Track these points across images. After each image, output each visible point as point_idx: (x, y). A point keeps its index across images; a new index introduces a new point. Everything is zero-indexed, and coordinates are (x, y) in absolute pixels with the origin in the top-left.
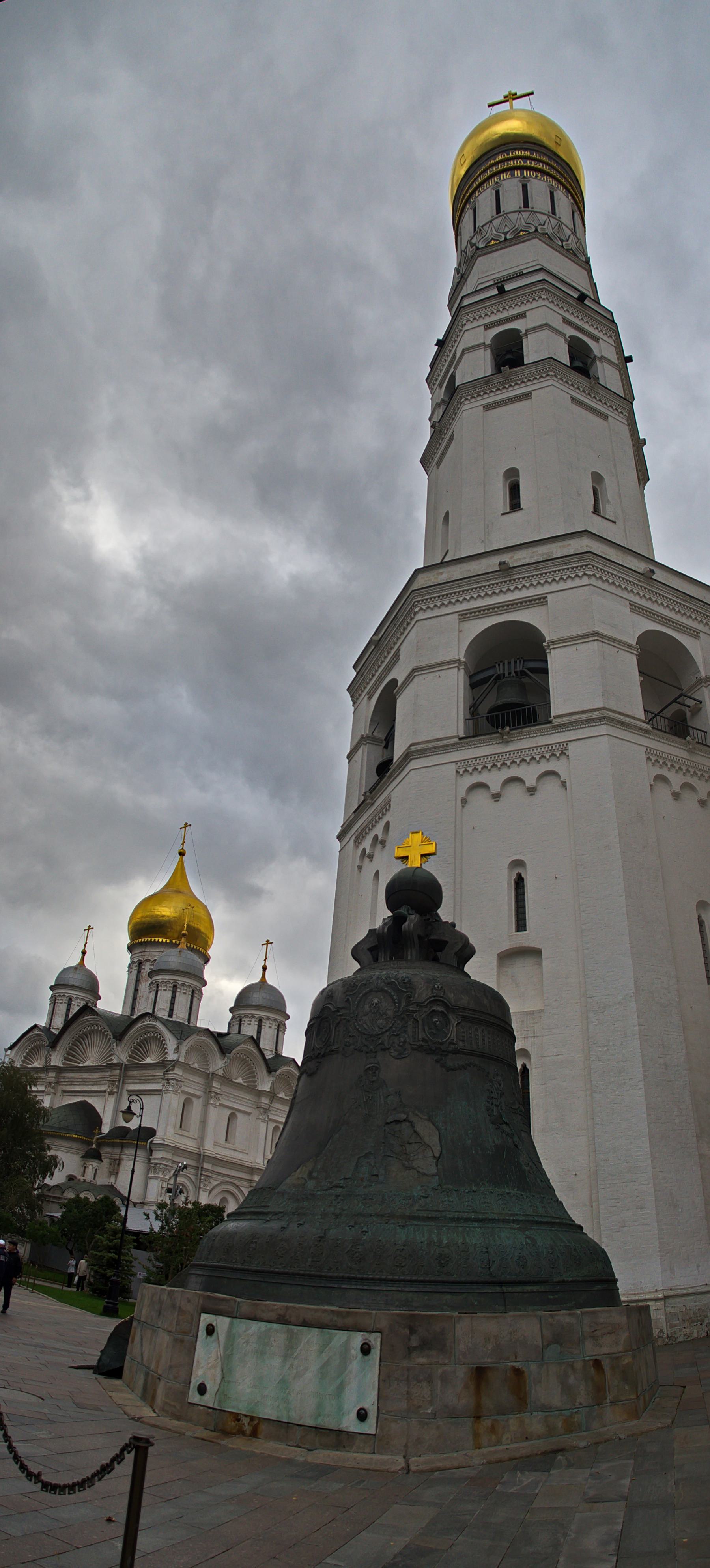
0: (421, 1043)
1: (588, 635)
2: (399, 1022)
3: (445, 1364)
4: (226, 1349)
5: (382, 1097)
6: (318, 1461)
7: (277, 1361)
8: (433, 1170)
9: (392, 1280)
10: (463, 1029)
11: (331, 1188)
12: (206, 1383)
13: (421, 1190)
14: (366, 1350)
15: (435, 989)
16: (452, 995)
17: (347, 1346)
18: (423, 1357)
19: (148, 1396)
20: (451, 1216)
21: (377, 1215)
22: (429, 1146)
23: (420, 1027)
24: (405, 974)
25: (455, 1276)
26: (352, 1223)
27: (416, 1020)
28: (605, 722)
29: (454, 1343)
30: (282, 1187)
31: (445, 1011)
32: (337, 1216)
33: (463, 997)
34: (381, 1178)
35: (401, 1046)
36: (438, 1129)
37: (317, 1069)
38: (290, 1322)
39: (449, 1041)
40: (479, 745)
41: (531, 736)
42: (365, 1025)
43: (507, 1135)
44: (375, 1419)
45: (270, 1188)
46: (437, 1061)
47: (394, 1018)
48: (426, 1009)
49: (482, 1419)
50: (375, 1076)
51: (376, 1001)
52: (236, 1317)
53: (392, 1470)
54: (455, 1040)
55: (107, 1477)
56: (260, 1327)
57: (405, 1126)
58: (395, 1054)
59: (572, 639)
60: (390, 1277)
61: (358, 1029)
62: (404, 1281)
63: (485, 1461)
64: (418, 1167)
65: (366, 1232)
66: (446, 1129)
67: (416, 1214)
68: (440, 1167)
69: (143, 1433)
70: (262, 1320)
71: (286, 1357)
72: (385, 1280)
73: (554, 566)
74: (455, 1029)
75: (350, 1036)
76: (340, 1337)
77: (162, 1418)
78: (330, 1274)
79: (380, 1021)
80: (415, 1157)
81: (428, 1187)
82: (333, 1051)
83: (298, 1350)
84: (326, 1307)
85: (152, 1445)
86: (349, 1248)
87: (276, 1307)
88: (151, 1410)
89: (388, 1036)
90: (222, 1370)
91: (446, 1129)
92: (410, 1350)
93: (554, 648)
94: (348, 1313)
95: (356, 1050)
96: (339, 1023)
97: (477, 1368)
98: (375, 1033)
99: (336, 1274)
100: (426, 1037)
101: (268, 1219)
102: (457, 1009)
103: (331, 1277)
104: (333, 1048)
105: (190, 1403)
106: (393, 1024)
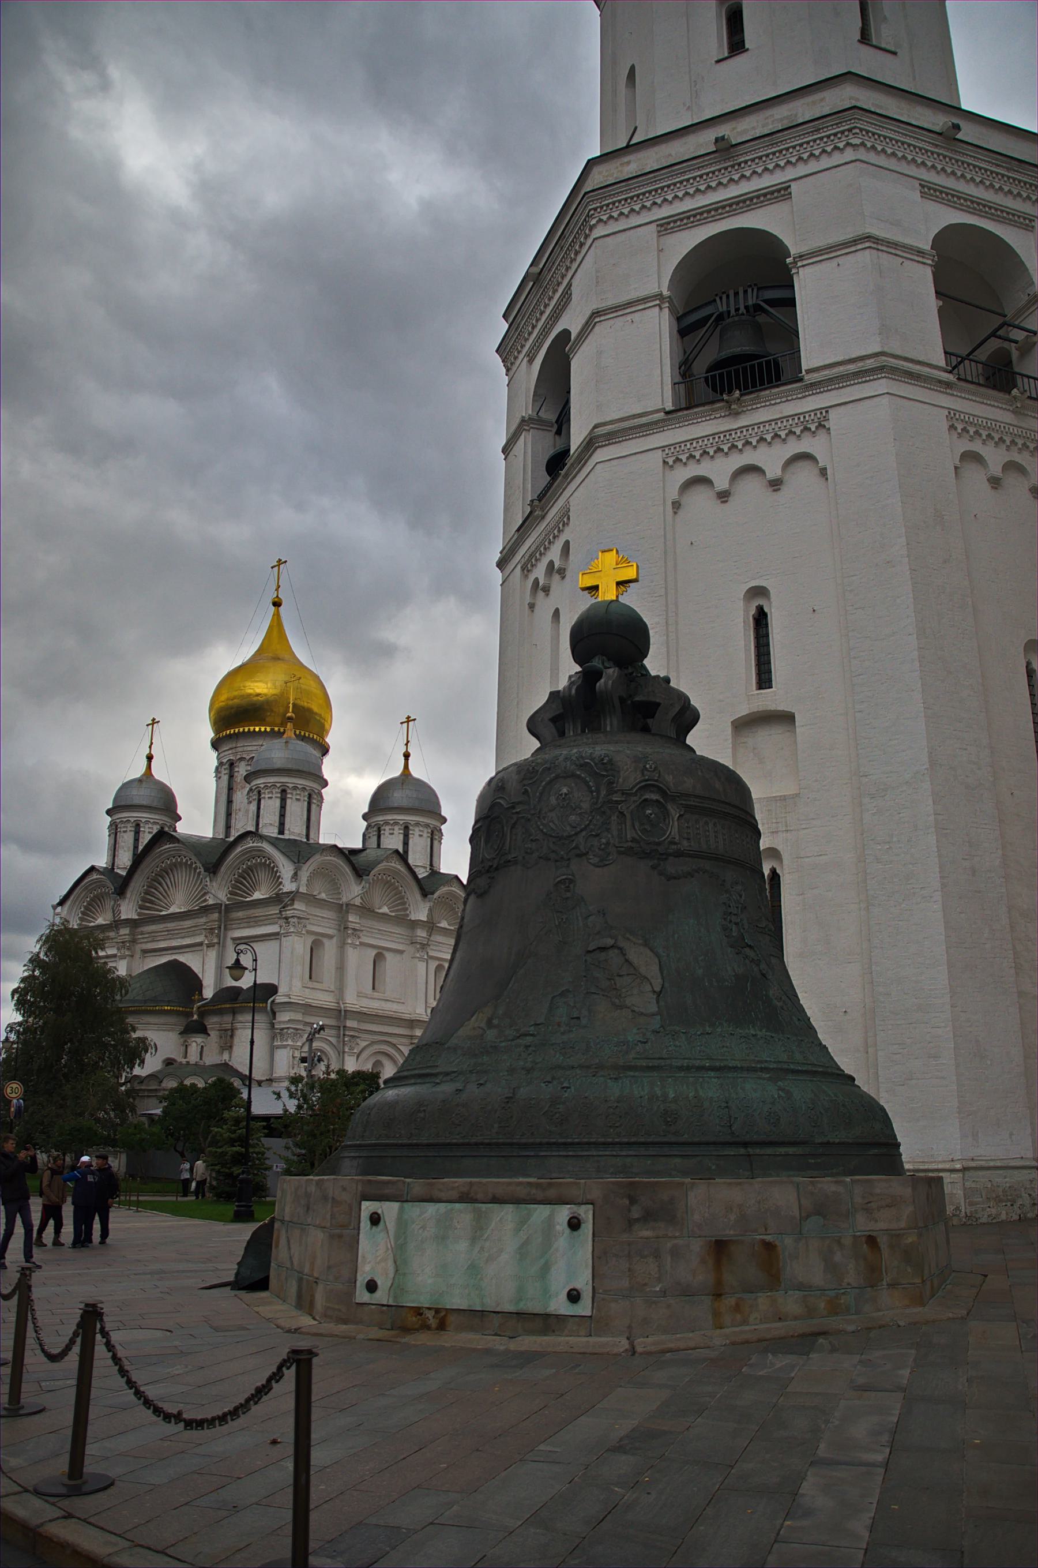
0: (630, 844)
1: (855, 242)
3: (676, 1237)
4: (397, 1237)
5: (580, 918)
6: (523, 1349)
7: (463, 1246)
8: (654, 1008)
9: (604, 1144)
10: (688, 823)
11: (518, 1037)
12: (376, 1279)
13: (637, 1034)
14: (574, 1224)
16: (671, 777)
17: (550, 1222)
19: (304, 1303)
20: (679, 1064)
21: (581, 1067)
22: (646, 978)
23: (629, 823)
24: (604, 752)
25: (686, 1136)
26: (548, 1078)
27: (622, 813)
28: (883, 375)
29: (687, 1212)
30: (454, 1041)
31: (662, 800)
32: (529, 1071)
33: (686, 779)
34: (584, 1021)
35: (603, 850)
36: (657, 955)
37: (490, 887)
38: (476, 1200)
41: (773, 402)
42: (551, 824)
43: (751, 962)
44: (591, 1300)
45: (437, 1043)
46: (653, 867)
47: (591, 812)
48: (635, 798)
49: (723, 1297)
50: (569, 891)
51: (565, 790)
52: (407, 1201)
53: (614, 1352)
54: (677, 838)
55: (265, 1398)
56: (438, 1209)
57: (613, 953)
58: (596, 860)
60: (602, 1140)
61: (542, 831)
62: (620, 1143)
63: (728, 1341)
64: (633, 1005)
65: (568, 1088)
66: (668, 956)
67: (633, 1064)
68: (662, 1003)
69: (303, 1344)
70: (440, 1201)
71: (474, 1240)
72: (594, 1143)
73: (799, 136)
74: (676, 823)
75: (532, 840)
76: (541, 1212)
77: (325, 1325)
78: (524, 1141)
79: (573, 817)
80: (629, 993)
81: (647, 1029)
82: (509, 861)
83: (489, 1232)
84: (521, 1179)
85: (317, 1355)
86: (546, 1109)
87: (457, 1184)
88: (310, 1318)
90: (395, 1262)
91: (668, 956)
92: (631, 1223)
93: (803, 266)
94: (550, 1184)
96: (515, 823)
97: (716, 1241)
98: (565, 834)
99: (531, 1140)
101: (438, 1081)
103: (525, 1144)
104: (509, 857)
105: (357, 1303)
106: (591, 821)
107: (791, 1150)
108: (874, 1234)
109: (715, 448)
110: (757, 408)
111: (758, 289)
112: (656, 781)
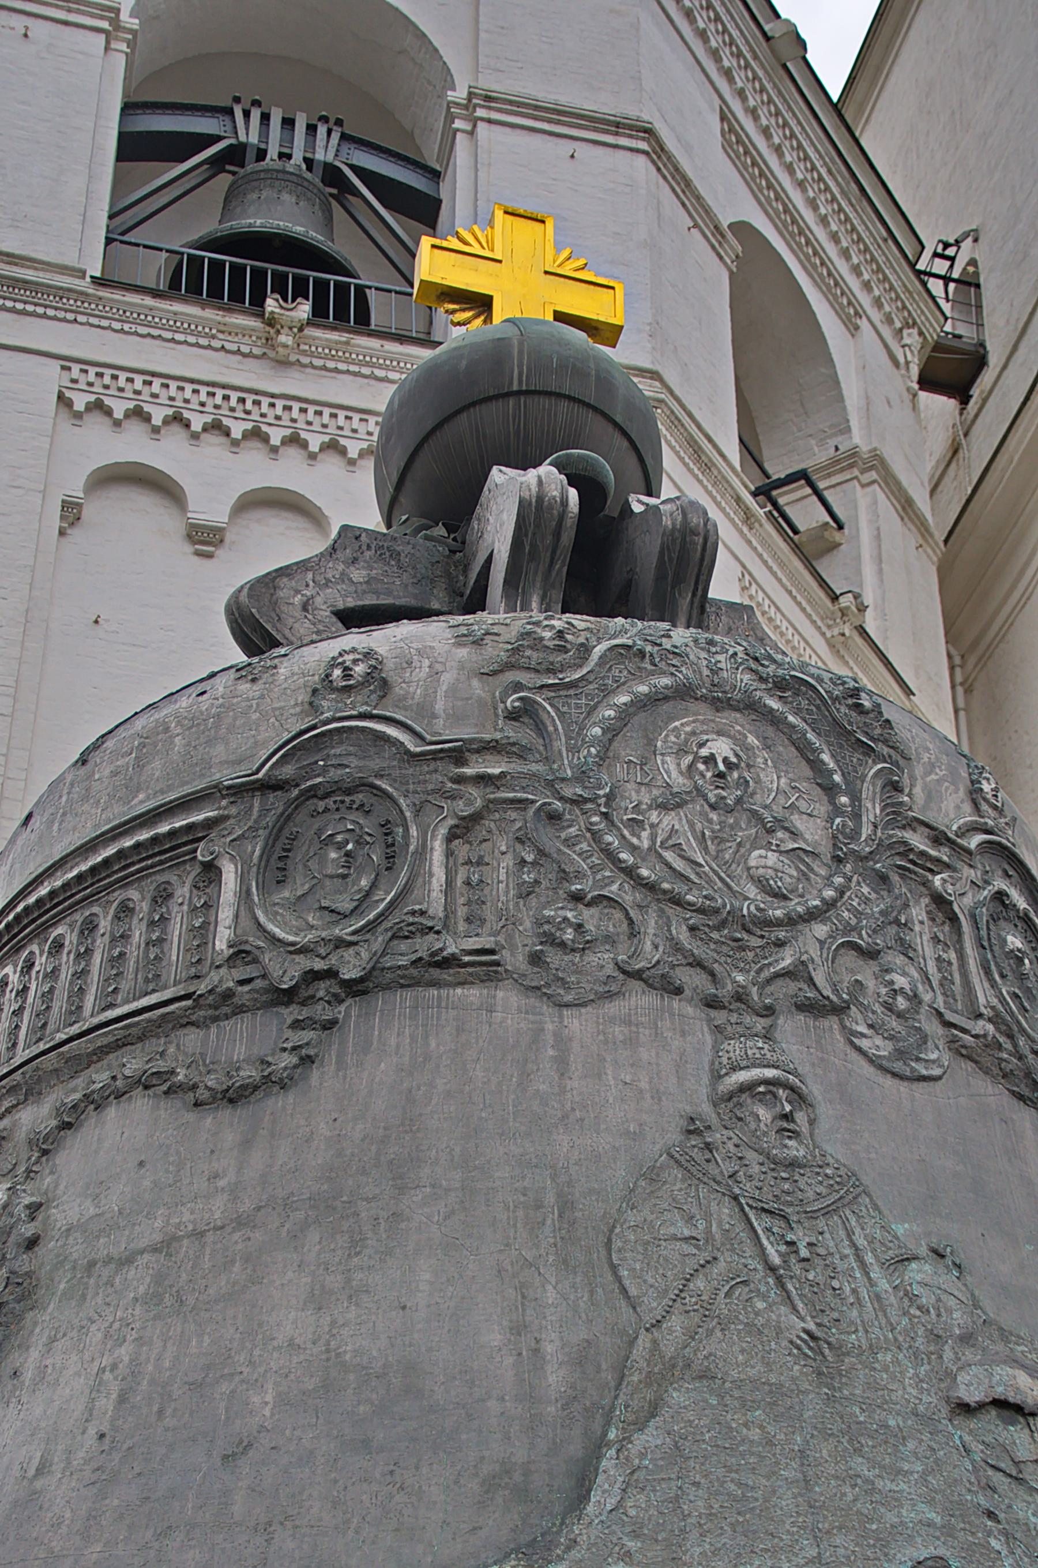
1: (618, 126)
2: (865, 890)
40: (168, 335)
47: (838, 860)
50: (795, 1134)
51: (721, 748)
59: (559, 114)
75: (577, 898)
79: (772, 858)
82: (448, 962)
89: (822, 943)
93: (490, 121)
95: (638, 975)
96: (476, 818)
109: (209, 419)
110: (336, 370)
111: (344, 137)
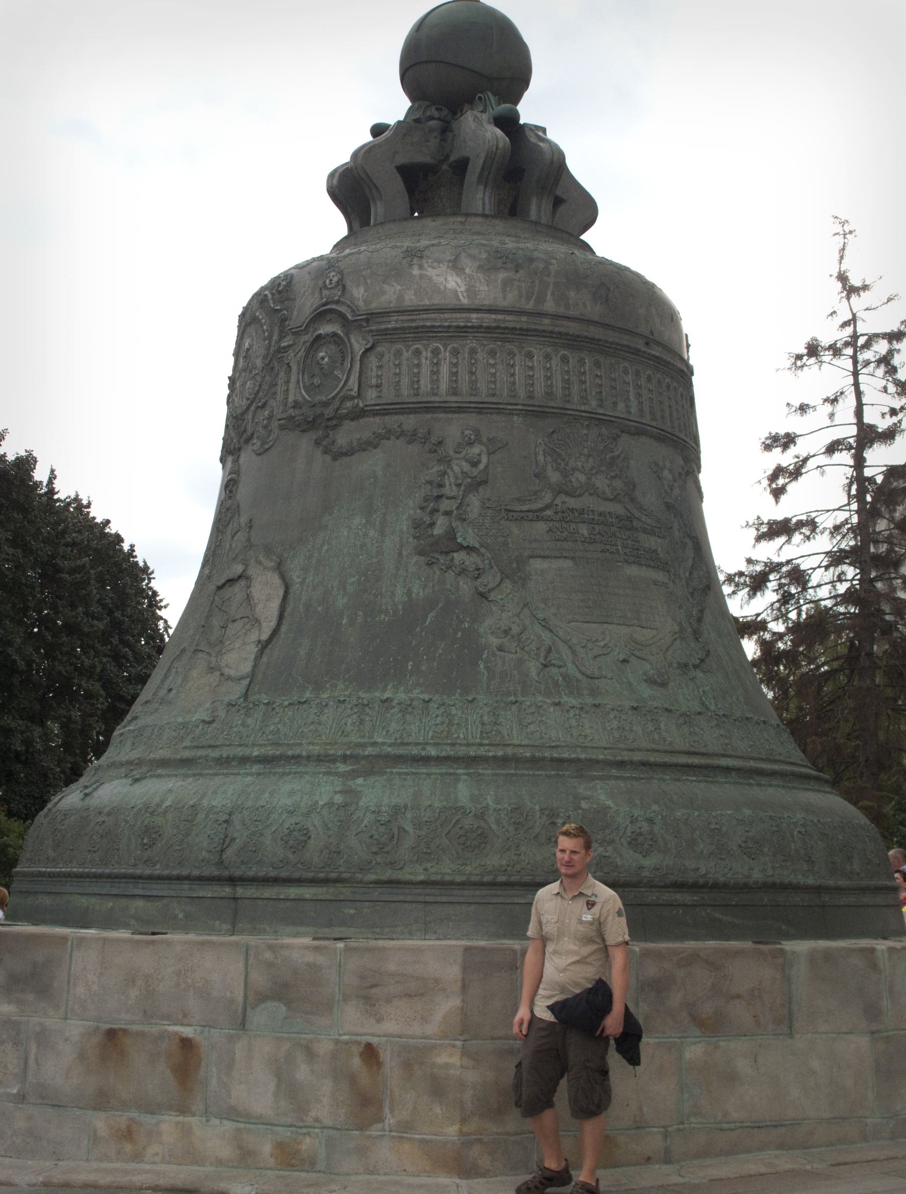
15: (325, 287)
16: (362, 290)
18: (9, 1003)
31: (339, 332)
39: (341, 394)
100: (300, 399)
102: (367, 320)
107: (308, 892)
108: (374, 1040)
112: (338, 302)
